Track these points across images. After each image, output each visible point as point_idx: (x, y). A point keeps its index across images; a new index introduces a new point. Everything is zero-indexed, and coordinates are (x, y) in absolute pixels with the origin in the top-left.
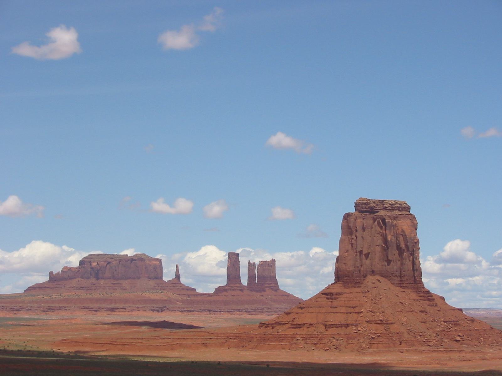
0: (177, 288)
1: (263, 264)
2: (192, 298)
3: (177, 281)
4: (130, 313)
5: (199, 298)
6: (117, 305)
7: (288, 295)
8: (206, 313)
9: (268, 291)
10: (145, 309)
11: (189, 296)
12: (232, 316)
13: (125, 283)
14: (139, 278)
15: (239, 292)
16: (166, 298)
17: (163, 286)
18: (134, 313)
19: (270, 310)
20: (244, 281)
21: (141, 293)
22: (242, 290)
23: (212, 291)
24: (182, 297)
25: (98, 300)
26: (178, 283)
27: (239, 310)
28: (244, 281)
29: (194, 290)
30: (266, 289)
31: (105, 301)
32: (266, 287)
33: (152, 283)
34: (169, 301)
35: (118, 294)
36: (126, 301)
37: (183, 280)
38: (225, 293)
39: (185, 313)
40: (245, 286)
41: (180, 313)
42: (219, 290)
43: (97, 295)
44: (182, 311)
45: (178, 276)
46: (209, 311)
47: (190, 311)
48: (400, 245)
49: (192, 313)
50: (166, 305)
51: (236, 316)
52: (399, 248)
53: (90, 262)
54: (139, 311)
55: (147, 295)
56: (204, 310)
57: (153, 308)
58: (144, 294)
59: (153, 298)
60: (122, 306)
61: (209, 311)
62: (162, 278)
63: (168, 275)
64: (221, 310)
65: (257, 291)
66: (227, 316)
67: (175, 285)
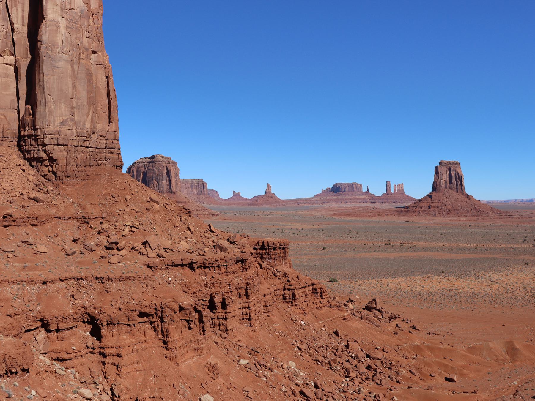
2: (373, 198)
5: (376, 198)
6: (347, 201)
7: (408, 196)
13: (349, 193)
14: (354, 191)
15: (391, 195)
17: (363, 194)
20: (392, 192)
25: (341, 199)
28: (392, 192)
31: (343, 199)
34: (365, 199)
35: (347, 197)
36: (351, 199)
41: (370, 203)
42: (383, 195)
43: (340, 197)
45: (368, 190)
51: (390, 204)
52: (456, 179)
53: (336, 186)
55: (357, 197)
63: (364, 190)
66: (387, 204)
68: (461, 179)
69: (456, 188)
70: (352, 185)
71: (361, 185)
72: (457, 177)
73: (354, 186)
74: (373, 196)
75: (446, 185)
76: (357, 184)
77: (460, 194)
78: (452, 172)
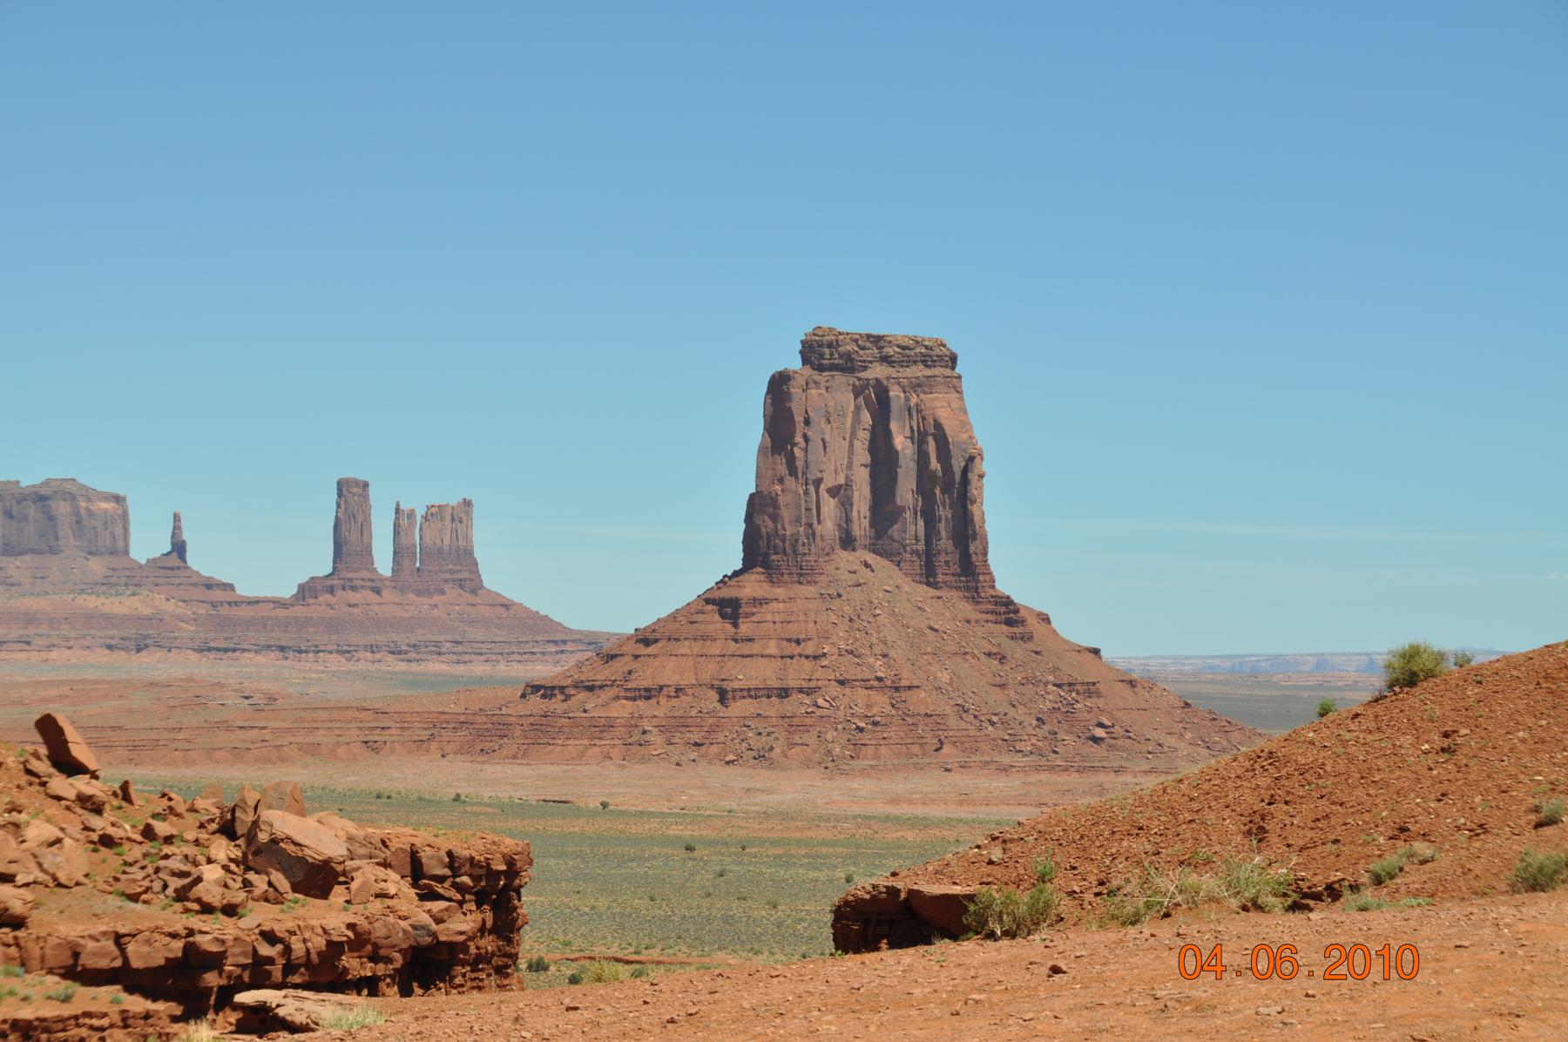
0: (178, 581)
1: (435, 513)
2: (225, 611)
3: (174, 561)
4: (44, 655)
7: (507, 605)
8: (272, 655)
9: (452, 593)
10: (86, 643)
11: (213, 604)
12: (352, 666)
14: (53, 551)
15: (372, 597)
16: (147, 611)
17: (136, 578)
18: (55, 654)
19: (460, 648)
20: (383, 562)
21: (71, 596)
22: (377, 591)
23: (288, 591)
24: (195, 609)
26: (179, 568)
27: (372, 649)
28: (383, 562)
29: (229, 587)
30: (447, 587)
32: (446, 581)
33: (97, 567)
34: (157, 619)
36: (30, 619)
37: (194, 560)
38: (325, 598)
39: (212, 655)
40: (387, 579)
41: (193, 656)
42: (307, 591)
44: (200, 651)
45: (179, 548)
46: (282, 649)
47: (226, 650)
48: (928, 463)
49: (230, 654)
50: (151, 632)
51: (364, 663)
54: (70, 648)
55: (91, 602)
56: (269, 647)
57: (109, 641)
58: (80, 600)
59: (108, 611)
60: (15, 632)
61: (282, 649)
62: (127, 552)
63: (147, 544)
64: (316, 646)
65: (419, 593)
66: (336, 663)
67: (169, 573)
68: (965, 481)
69: (921, 546)
70: (40, 497)
71: (118, 499)
72: (935, 464)
73: (62, 508)
74: (217, 595)
75: (848, 520)
76: (89, 494)
77: (955, 594)
78: (894, 426)
